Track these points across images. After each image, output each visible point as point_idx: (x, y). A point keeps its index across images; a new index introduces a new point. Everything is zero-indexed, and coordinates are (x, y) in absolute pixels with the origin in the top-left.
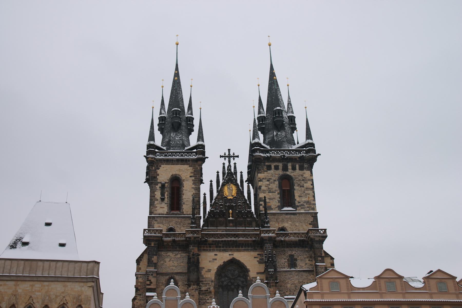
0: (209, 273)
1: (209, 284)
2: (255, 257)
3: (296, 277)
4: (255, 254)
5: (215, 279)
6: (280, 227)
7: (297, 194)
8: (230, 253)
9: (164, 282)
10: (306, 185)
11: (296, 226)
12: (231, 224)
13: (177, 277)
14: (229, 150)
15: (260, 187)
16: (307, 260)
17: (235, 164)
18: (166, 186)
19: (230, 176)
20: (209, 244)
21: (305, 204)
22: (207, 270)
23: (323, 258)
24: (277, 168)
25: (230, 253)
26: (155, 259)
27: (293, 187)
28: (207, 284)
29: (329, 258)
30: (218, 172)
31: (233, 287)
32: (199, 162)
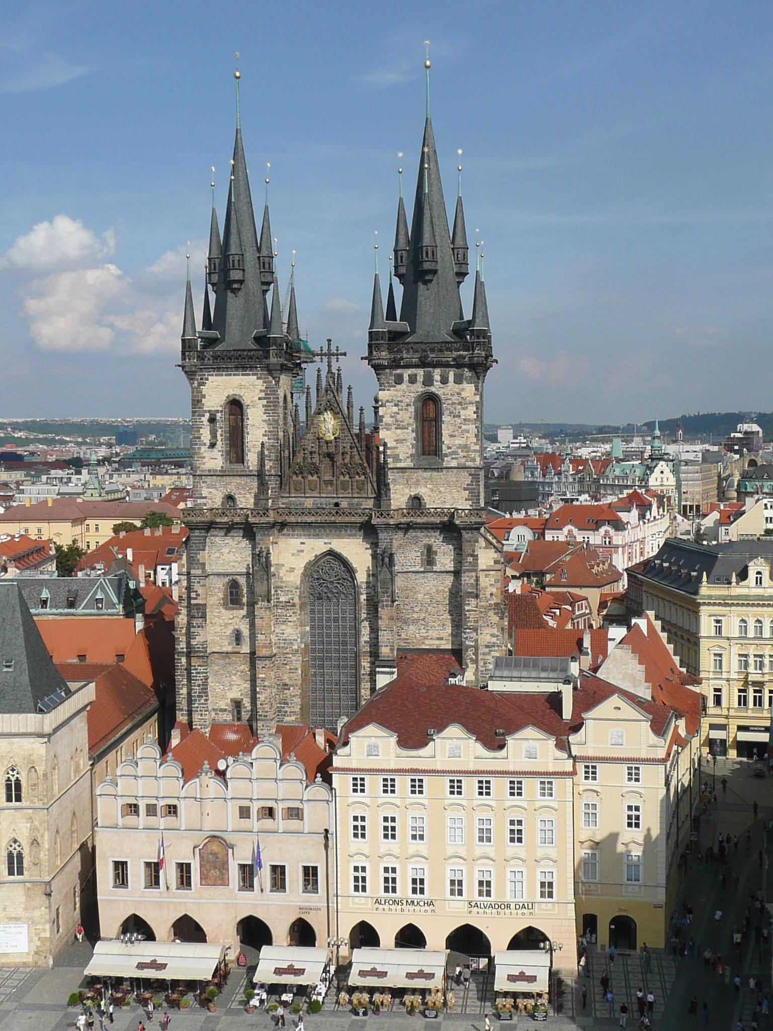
2: (367, 549)
6: (413, 494)
7: (445, 432)
8: (326, 541)
10: (463, 412)
11: (440, 492)
12: (330, 488)
13: (242, 581)
14: (329, 341)
15: (382, 416)
18: (218, 418)
21: (460, 450)
23: (475, 557)
24: (413, 380)
25: (326, 541)
26: (203, 556)
29: (493, 550)
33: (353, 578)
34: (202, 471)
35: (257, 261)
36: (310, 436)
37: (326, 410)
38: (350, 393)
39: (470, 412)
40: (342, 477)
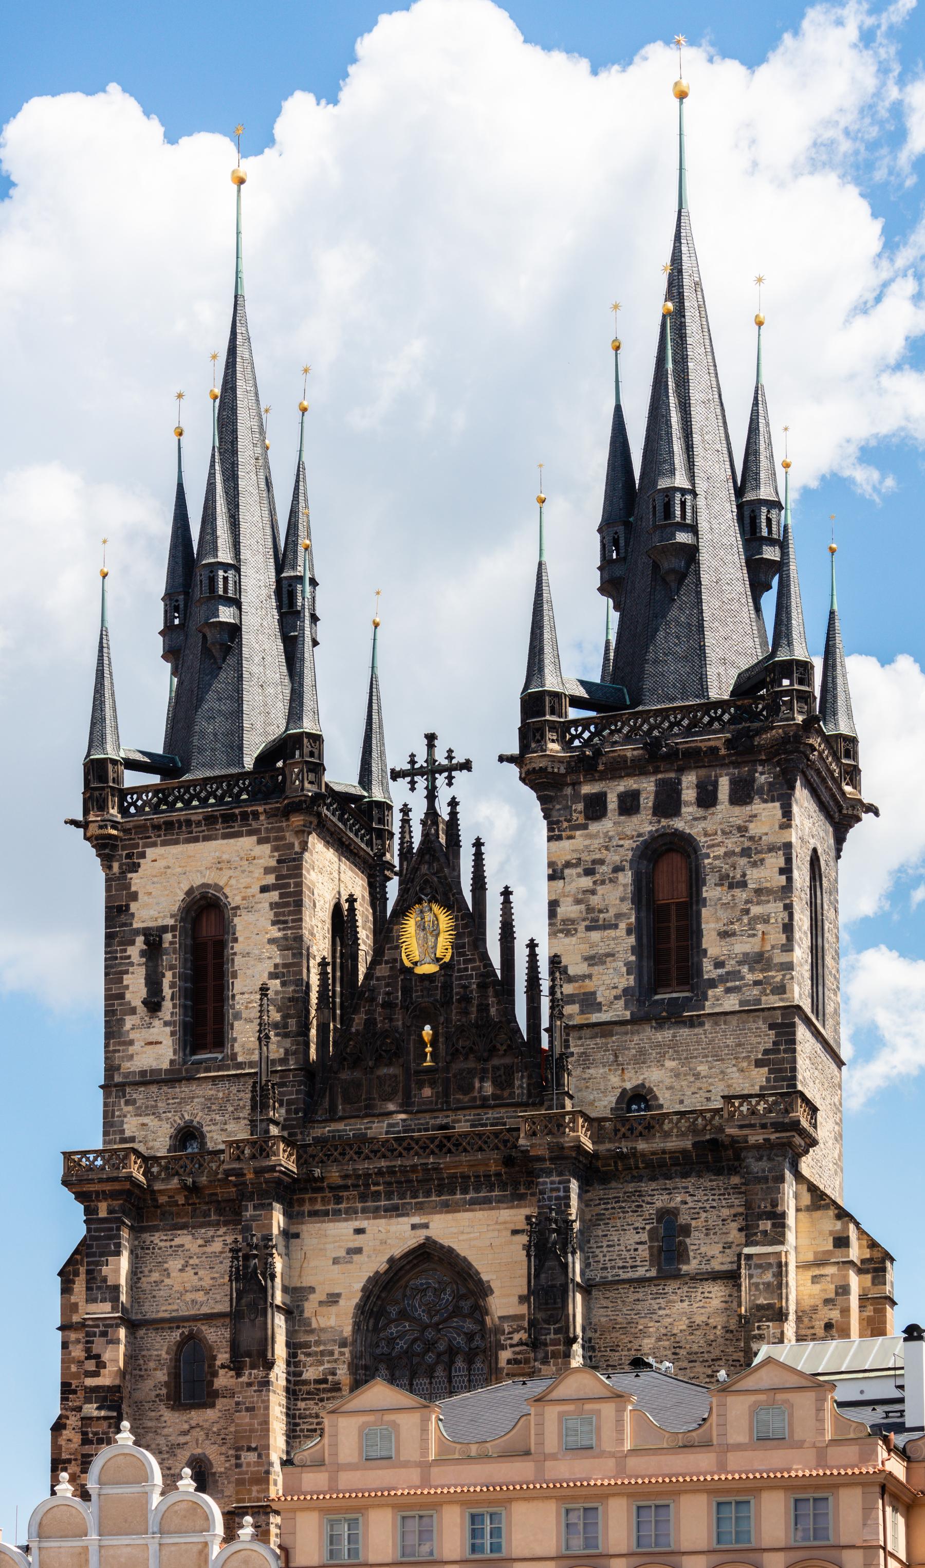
0: (333, 1309)
1: (331, 1353)
2: (515, 1232)
3: (679, 1305)
4: (517, 1215)
5: (353, 1332)
6: (628, 1086)
7: (711, 922)
8: (416, 1220)
9: (163, 1353)
11: (697, 1076)
12: (427, 1092)
14: (431, 738)
16: (734, 1226)
17: (453, 803)
18: (166, 945)
20: (332, 1188)
21: (745, 970)
22: (324, 1298)
24: (629, 805)
25: (416, 1220)
27: (699, 892)
28: (322, 1353)
31: (430, 1358)
32: (297, 820)
33: (485, 1311)
34: (127, 1075)
36: (382, 970)
37: (420, 901)
38: (479, 858)
40: (459, 1065)
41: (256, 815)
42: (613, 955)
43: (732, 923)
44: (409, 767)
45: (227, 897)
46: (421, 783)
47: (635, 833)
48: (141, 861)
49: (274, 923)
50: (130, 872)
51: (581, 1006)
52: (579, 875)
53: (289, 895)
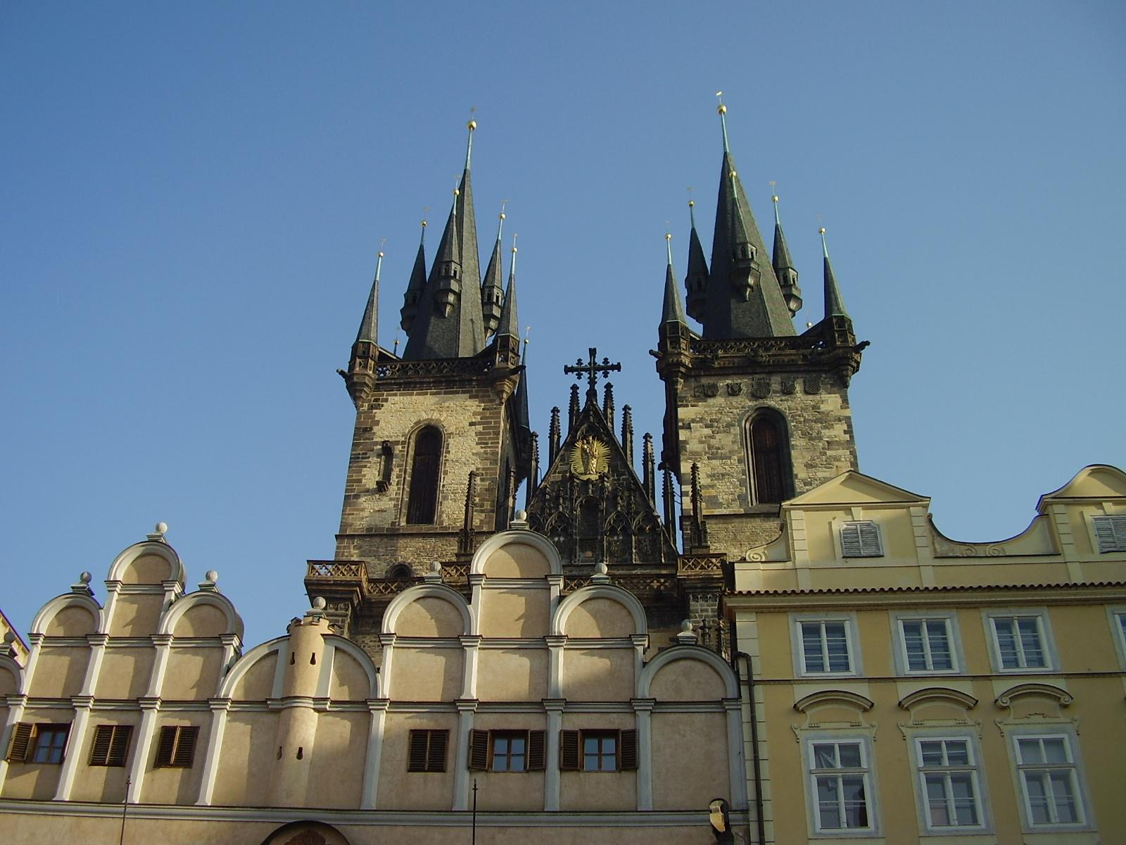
12: (589, 554)
14: (593, 352)
15: (685, 442)
17: (609, 386)
18: (397, 452)
19: (590, 420)
24: (733, 392)
30: (555, 411)
35: (479, 291)
37: (584, 437)
39: (838, 431)
41: (471, 381)
42: (729, 475)
43: (814, 460)
44: (575, 366)
45: (444, 427)
46: (585, 375)
47: (740, 406)
48: (384, 403)
49: (477, 444)
50: (377, 409)
51: (707, 504)
52: (701, 427)
53: (490, 428)
